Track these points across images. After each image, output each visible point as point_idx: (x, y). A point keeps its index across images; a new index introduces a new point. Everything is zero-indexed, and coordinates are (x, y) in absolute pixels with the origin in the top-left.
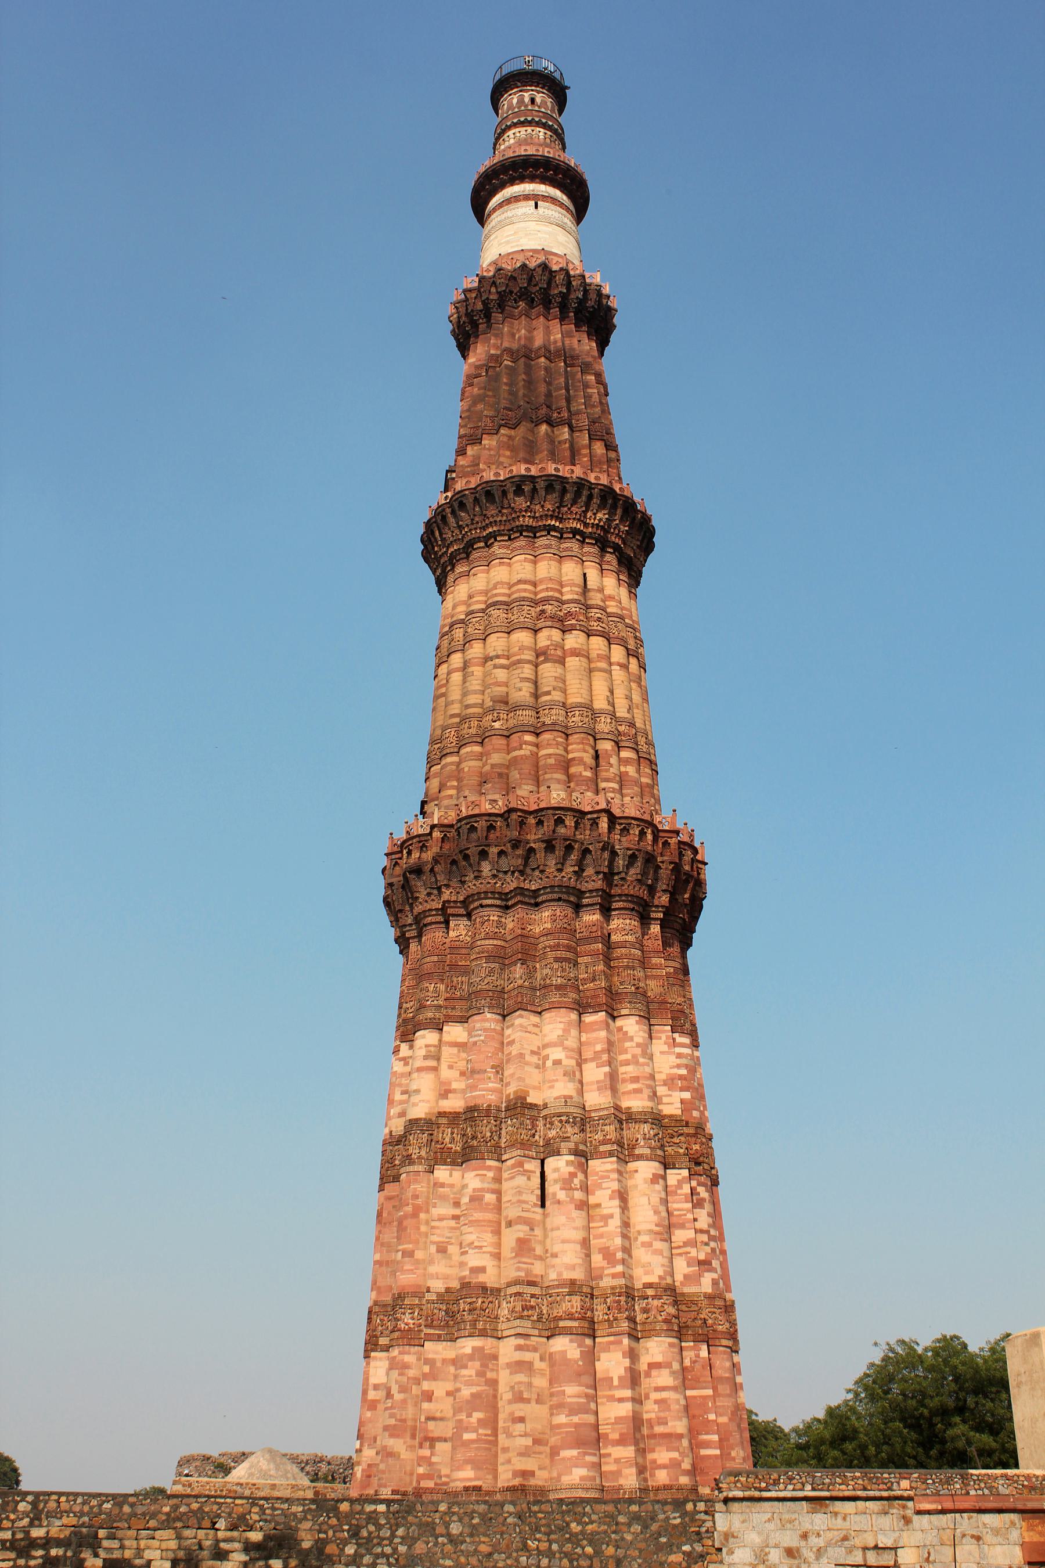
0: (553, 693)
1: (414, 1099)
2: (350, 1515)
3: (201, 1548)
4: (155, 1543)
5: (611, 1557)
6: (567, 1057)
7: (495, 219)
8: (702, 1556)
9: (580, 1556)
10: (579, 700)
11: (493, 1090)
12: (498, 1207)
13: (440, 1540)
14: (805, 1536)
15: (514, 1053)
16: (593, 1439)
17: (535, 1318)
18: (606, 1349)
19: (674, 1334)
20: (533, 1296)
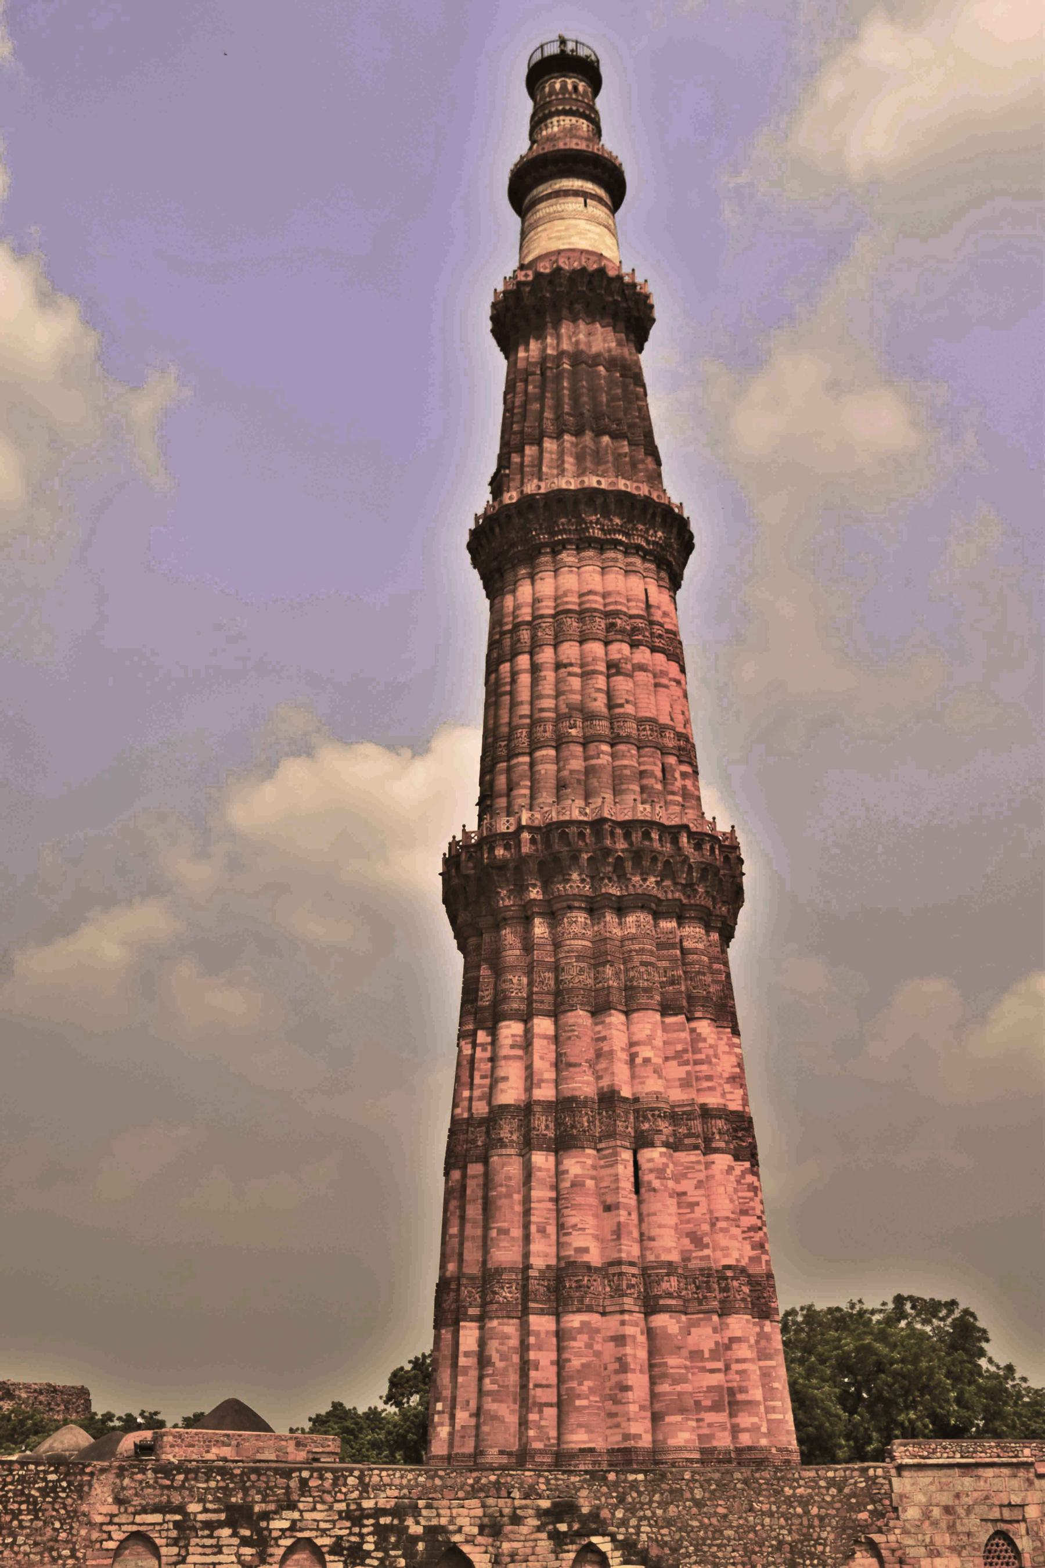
0: (627, 706)
1: (501, 1086)
2: (616, 1484)
3: (502, 1515)
5: (816, 1516)
6: (656, 1055)
7: (544, 209)
8: (883, 1516)
9: (793, 1515)
10: (648, 715)
11: (588, 1083)
13: (688, 1503)
14: (957, 1496)
15: (606, 1049)
17: (635, 1296)
18: (695, 1324)
20: (633, 1275)
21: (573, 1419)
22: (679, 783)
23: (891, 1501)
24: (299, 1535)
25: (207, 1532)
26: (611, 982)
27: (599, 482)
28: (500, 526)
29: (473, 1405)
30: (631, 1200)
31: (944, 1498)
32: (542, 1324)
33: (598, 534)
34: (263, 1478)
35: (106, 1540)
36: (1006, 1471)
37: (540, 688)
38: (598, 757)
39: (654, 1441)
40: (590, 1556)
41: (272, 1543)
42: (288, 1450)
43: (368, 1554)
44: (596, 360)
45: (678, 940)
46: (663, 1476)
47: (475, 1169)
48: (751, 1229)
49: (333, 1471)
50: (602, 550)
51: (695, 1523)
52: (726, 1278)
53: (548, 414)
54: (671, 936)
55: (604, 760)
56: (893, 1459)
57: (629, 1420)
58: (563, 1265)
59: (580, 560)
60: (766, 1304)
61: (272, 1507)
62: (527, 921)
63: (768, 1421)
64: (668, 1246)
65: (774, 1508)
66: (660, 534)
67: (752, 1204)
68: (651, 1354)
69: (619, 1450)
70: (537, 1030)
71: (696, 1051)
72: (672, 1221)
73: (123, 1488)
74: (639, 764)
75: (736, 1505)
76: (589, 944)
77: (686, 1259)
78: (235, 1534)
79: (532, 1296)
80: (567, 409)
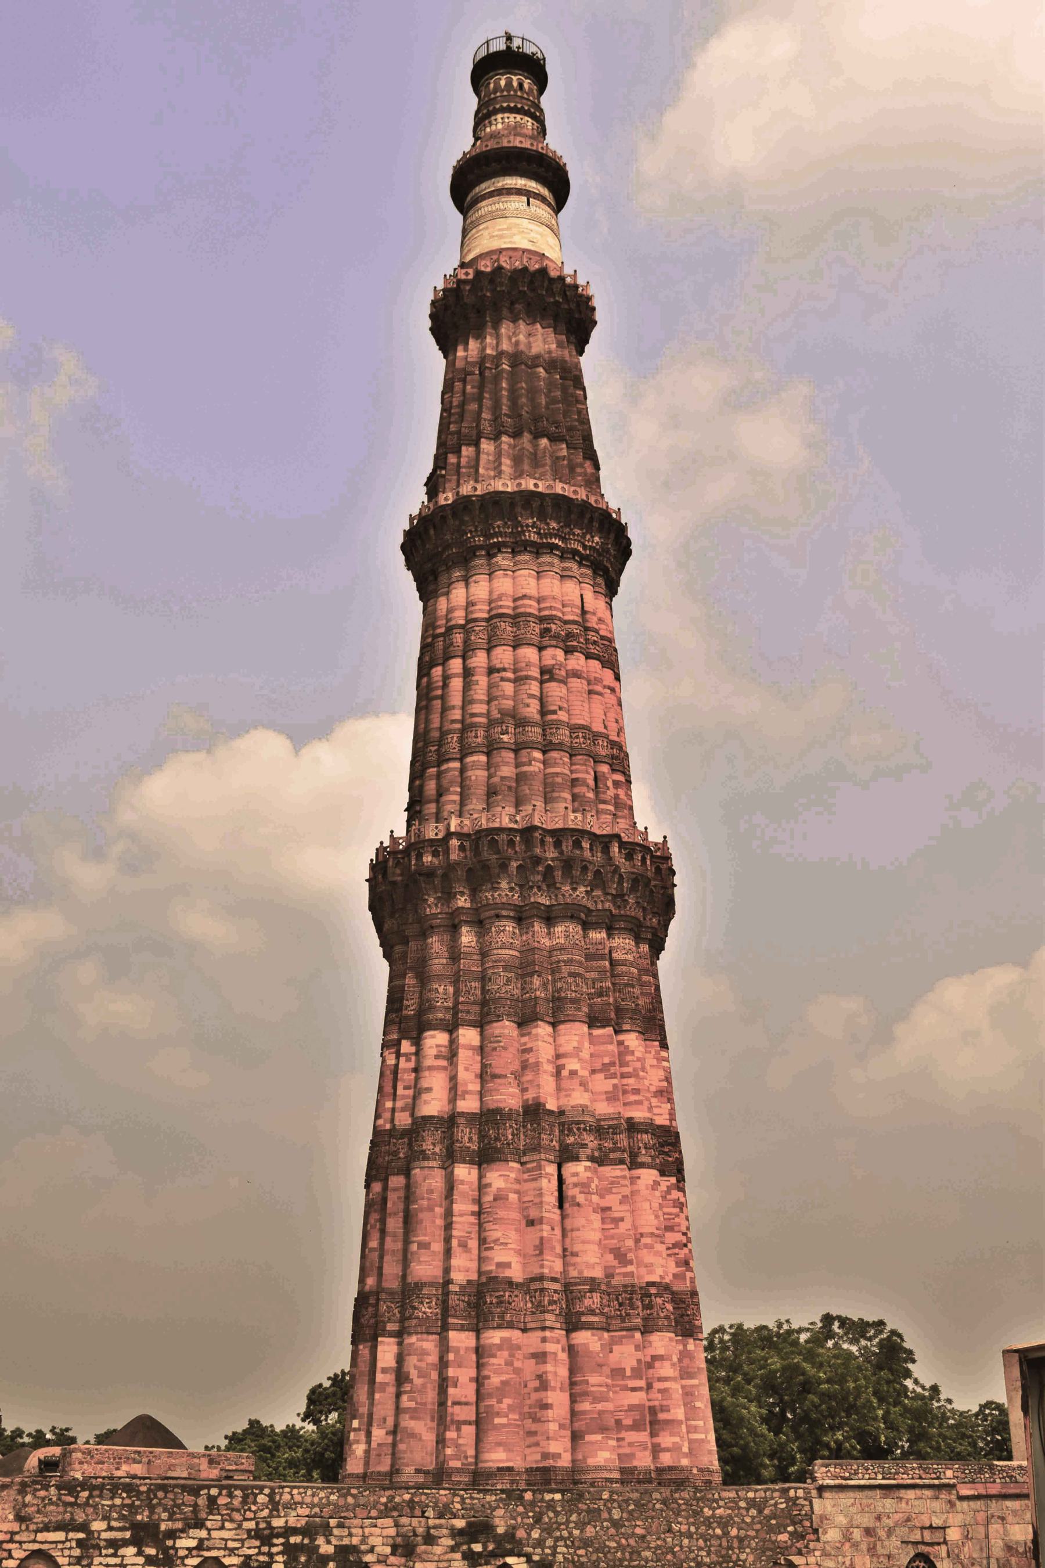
0: (559, 712)
1: (425, 1097)
2: (533, 1503)
3: (415, 1535)
4: (377, 1531)
6: (582, 1068)
7: (485, 207)
8: (802, 1537)
9: (712, 1537)
11: (512, 1095)
14: (879, 1518)
15: (531, 1061)
18: (620, 1341)
19: (672, 1329)
20: (555, 1291)
21: (491, 1438)
22: (611, 792)
23: (812, 1523)
24: (207, 1554)
25: (111, 1551)
26: (538, 993)
27: (536, 485)
28: (435, 527)
29: (390, 1422)
30: (555, 1215)
31: (865, 1520)
32: (461, 1340)
33: (534, 537)
34: (171, 1495)
35: (6, 1559)
36: (928, 1493)
37: (472, 692)
38: (530, 764)
39: (573, 1461)
41: (179, 1562)
42: (201, 1468)
44: (536, 361)
45: (607, 951)
46: (581, 1495)
47: (397, 1181)
48: (675, 1245)
49: (243, 1488)
50: (538, 554)
52: (650, 1295)
53: (486, 415)
54: (600, 947)
55: (536, 767)
56: (814, 1479)
57: (548, 1438)
58: (484, 1280)
59: (515, 564)
60: (690, 1322)
61: (179, 1525)
62: (454, 929)
63: (690, 1442)
64: (591, 1262)
65: (693, 1529)
66: (597, 539)
67: (677, 1220)
68: (572, 1371)
69: (537, 1469)
70: (462, 1040)
72: (596, 1236)
73: (25, 1505)
74: (572, 772)
75: (654, 1526)
76: (517, 954)
77: (609, 1276)
78: (140, 1553)
79: (452, 1312)
80: (505, 409)
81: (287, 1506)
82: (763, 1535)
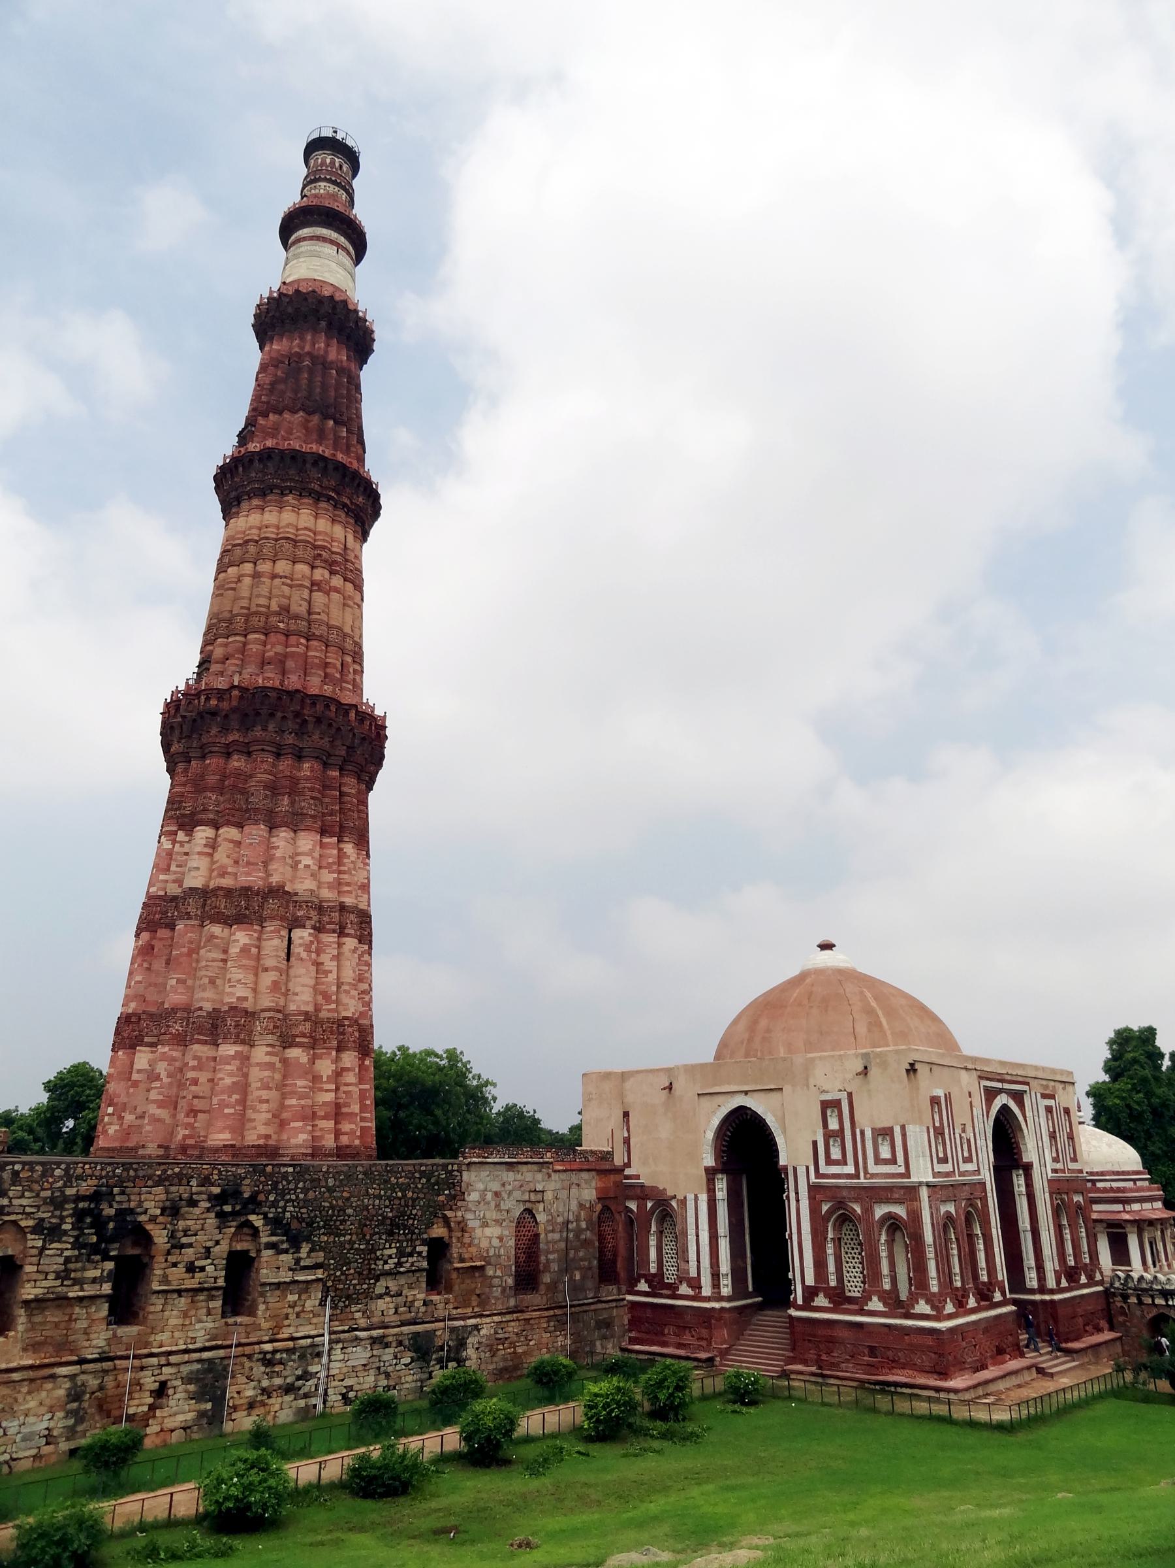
2: (272, 1174)
3: (181, 1199)
7: (305, 246)
8: (454, 1197)
11: (262, 878)
12: (258, 958)
14: (503, 1185)
16: (310, 1116)
21: (220, 1124)
22: (351, 676)
28: (243, 466)
33: (317, 488)
36: (535, 1167)
40: (245, 1230)
43: (65, 1232)
50: (318, 500)
51: (327, 1204)
66: (360, 499)
68: (285, 1077)
69: (253, 1146)
71: (340, 862)
77: (318, 1009)
81: (79, 1178)
82: (428, 1196)
